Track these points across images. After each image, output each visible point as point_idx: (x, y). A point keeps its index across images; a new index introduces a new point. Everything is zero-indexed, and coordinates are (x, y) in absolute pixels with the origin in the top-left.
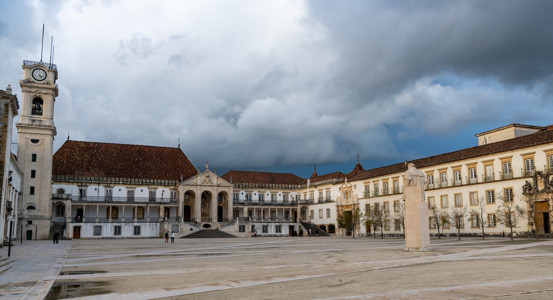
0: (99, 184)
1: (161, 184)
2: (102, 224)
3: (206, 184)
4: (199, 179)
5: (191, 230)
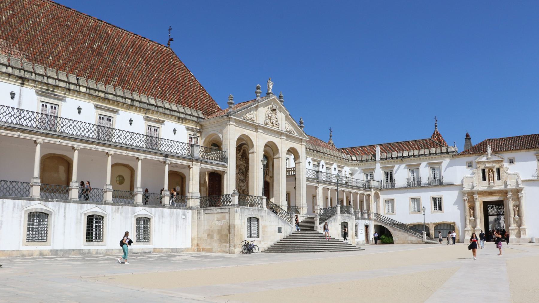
0: (23, 80)
1: (170, 114)
2: (50, 206)
3: (268, 127)
4: (261, 115)
5: (279, 230)
